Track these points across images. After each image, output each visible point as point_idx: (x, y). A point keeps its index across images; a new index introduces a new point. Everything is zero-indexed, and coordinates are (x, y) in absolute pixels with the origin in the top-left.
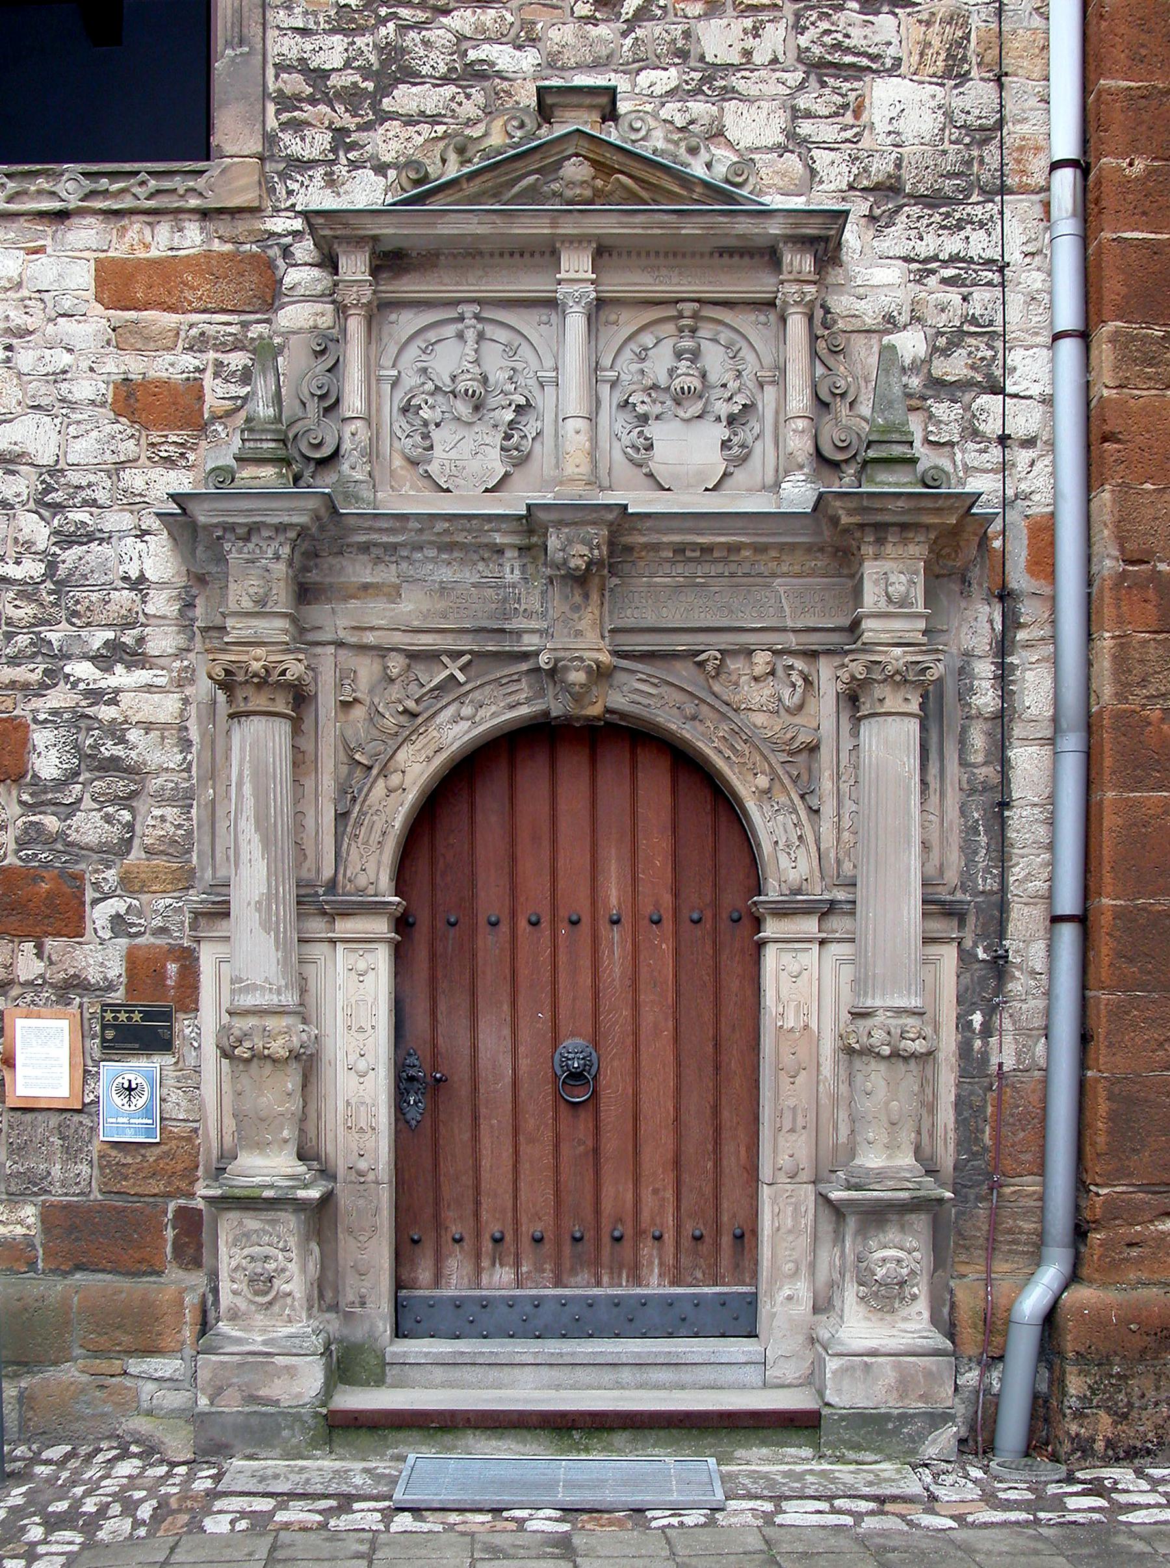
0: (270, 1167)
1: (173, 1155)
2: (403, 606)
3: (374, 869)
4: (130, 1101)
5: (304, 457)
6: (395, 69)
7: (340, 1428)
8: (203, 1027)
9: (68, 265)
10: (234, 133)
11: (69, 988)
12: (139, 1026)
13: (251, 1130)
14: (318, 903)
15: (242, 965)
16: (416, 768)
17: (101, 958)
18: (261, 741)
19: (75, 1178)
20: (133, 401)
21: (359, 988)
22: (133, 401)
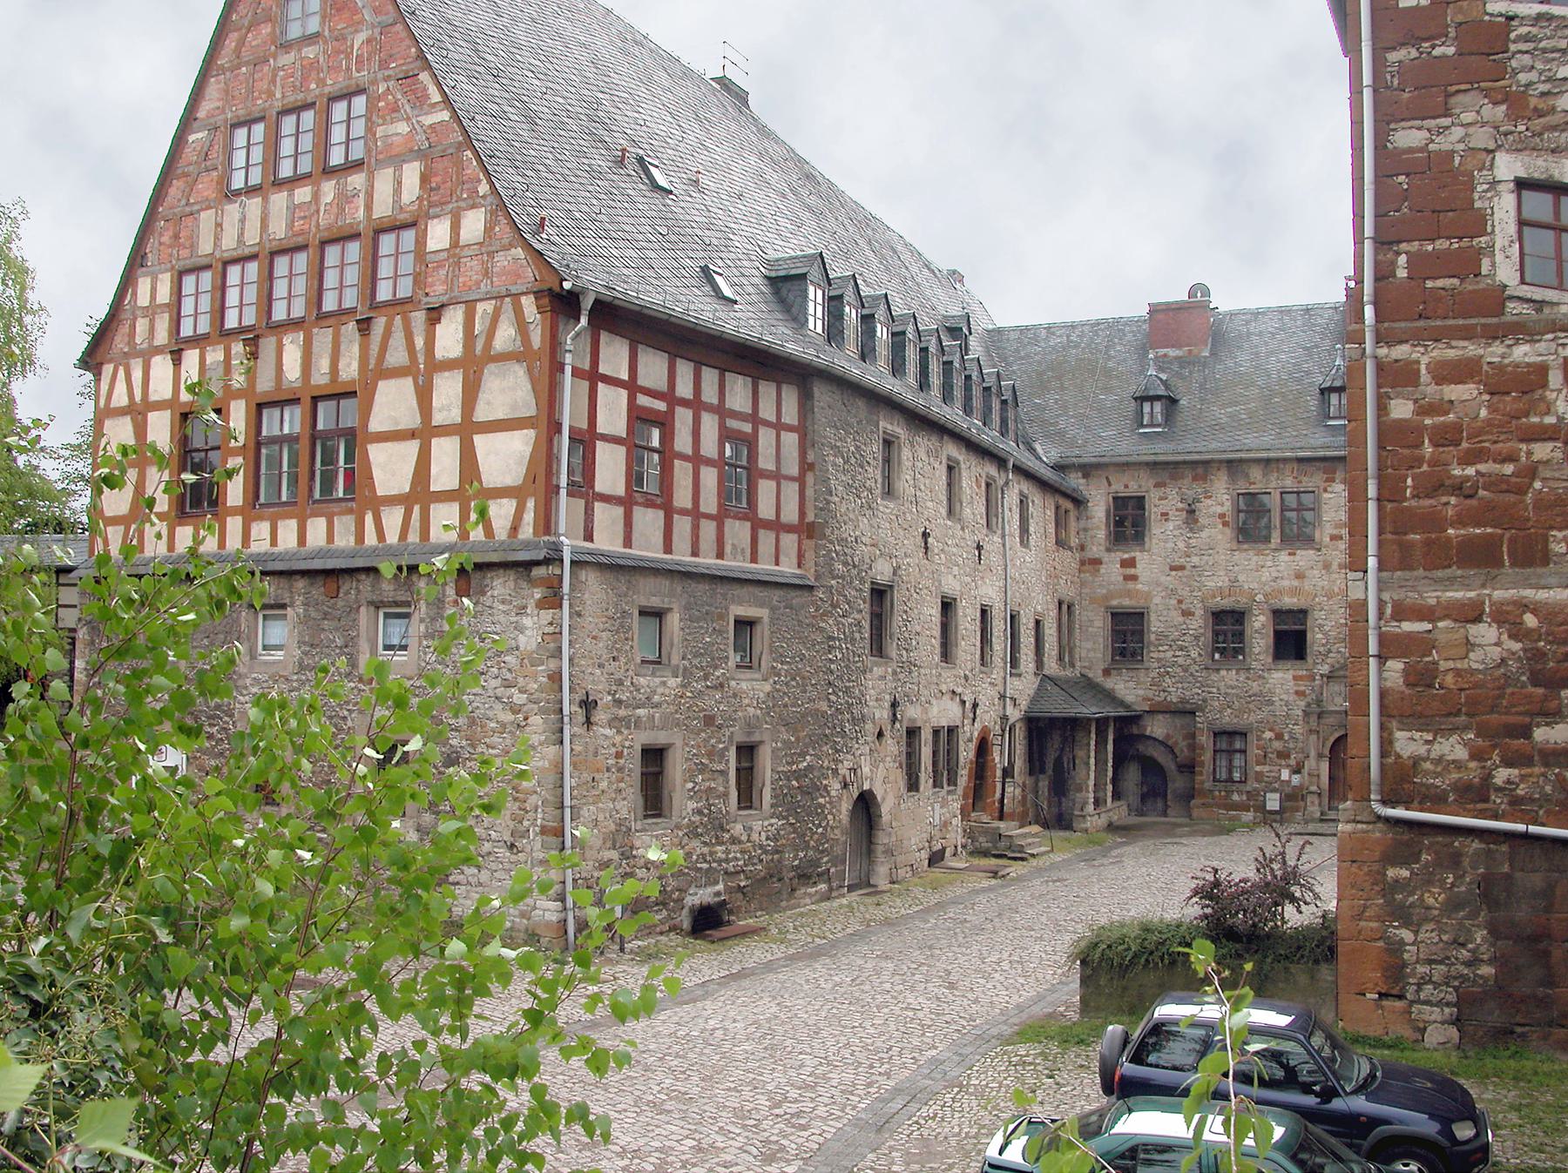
0: (1314, 788)
1: (1301, 788)
2: (1331, 720)
3: (1327, 752)
4: (1296, 779)
5: (1319, 702)
6: (1330, 651)
7: (1322, 820)
8: (1305, 771)
9: (1289, 675)
10: (1310, 660)
11: (1288, 766)
12: (1297, 770)
13: (1311, 783)
14: (1320, 756)
15: (1310, 764)
16: (1332, 739)
17: (1292, 762)
18: (1314, 737)
19: (1288, 790)
20: (1297, 693)
21: (1325, 767)
22: (1297, 693)
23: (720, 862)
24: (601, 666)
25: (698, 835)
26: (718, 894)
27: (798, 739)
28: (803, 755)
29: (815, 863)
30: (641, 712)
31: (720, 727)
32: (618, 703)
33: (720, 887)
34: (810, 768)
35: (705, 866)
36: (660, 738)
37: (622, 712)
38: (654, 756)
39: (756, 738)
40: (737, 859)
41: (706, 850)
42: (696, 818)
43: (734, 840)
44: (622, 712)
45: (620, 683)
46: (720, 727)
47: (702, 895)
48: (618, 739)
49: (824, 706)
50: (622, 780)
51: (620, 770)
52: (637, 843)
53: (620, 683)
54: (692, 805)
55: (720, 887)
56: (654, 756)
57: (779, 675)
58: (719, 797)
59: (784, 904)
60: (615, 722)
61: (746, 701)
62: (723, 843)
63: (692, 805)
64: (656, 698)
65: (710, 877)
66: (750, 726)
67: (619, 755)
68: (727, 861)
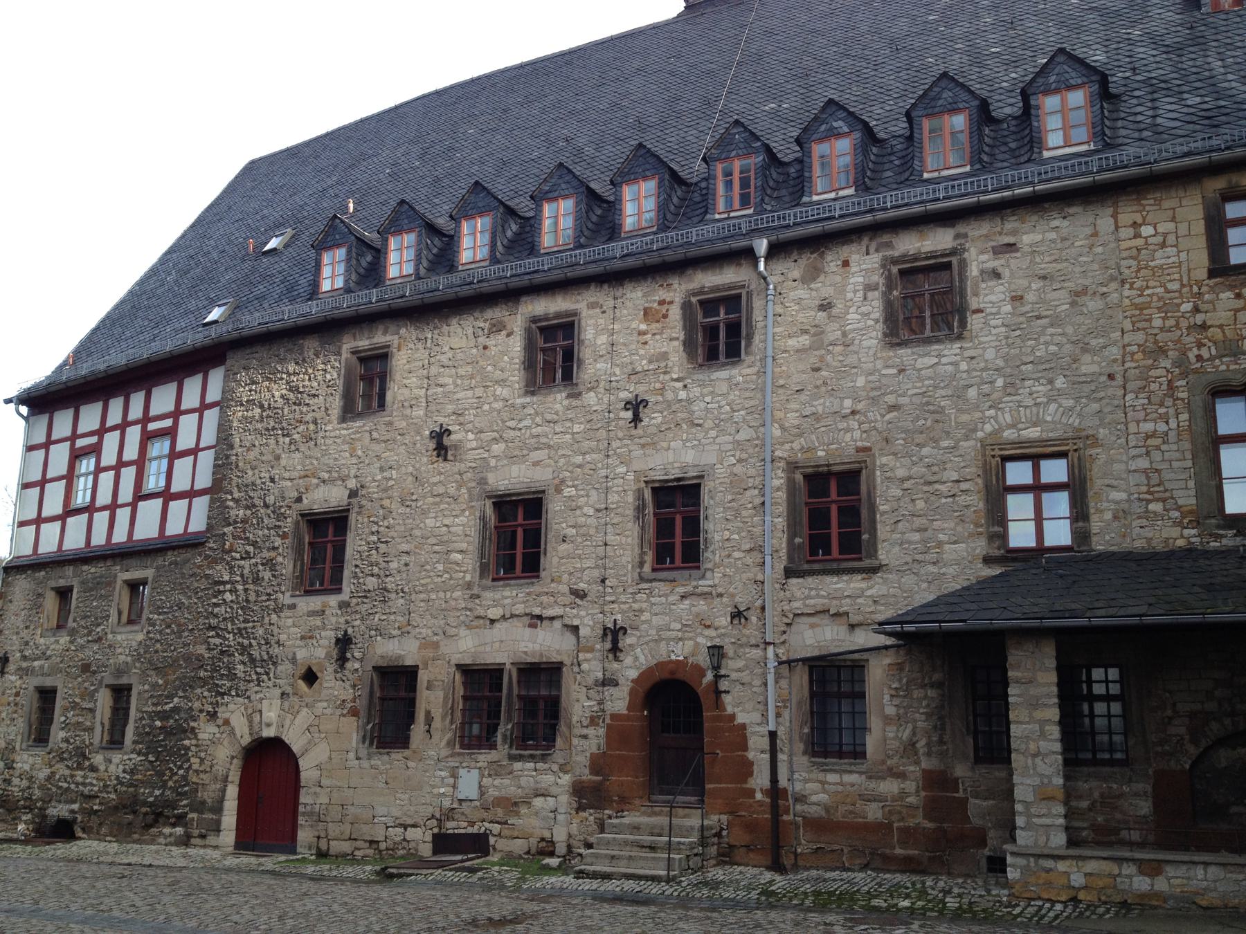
23: (77, 784)
24: (17, 633)
25: (62, 760)
26: (72, 811)
27: (166, 683)
28: (170, 697)
29: (173, 805)
30: (36, 663)
31: (94, 672)
32: (24, 658)
33: (76, 807)
34: (176, 710)
35: (65, 785)
36: (48, 682)
37: (25, 665)
38: (47, 696)
39: (124, 680)
40: (91, 784)
41: (67, 772)
42: (64, 745)
43: (93, 769)
44: (25, 665)
45: (27, 644)
46: (94, 672)
47: (59, 810)
48: (18, 683)
49: (201, 650)
50: (16, 712)
51: (16, 704)
52: (18, 758)
53: (27, 644)
54: (62, 734)
55: (76, 807)
56: (47, 696)
57: (154, 625)
58: (84, 730)
59: (136, 836)
60: (23, 672)
61: (120, 650)
62: (82, 769)
63: (62, 734)
64: (49, 653)
65: (65, 795)
66: (119, 672)
67: (17, 694)
68: (84, 784)
